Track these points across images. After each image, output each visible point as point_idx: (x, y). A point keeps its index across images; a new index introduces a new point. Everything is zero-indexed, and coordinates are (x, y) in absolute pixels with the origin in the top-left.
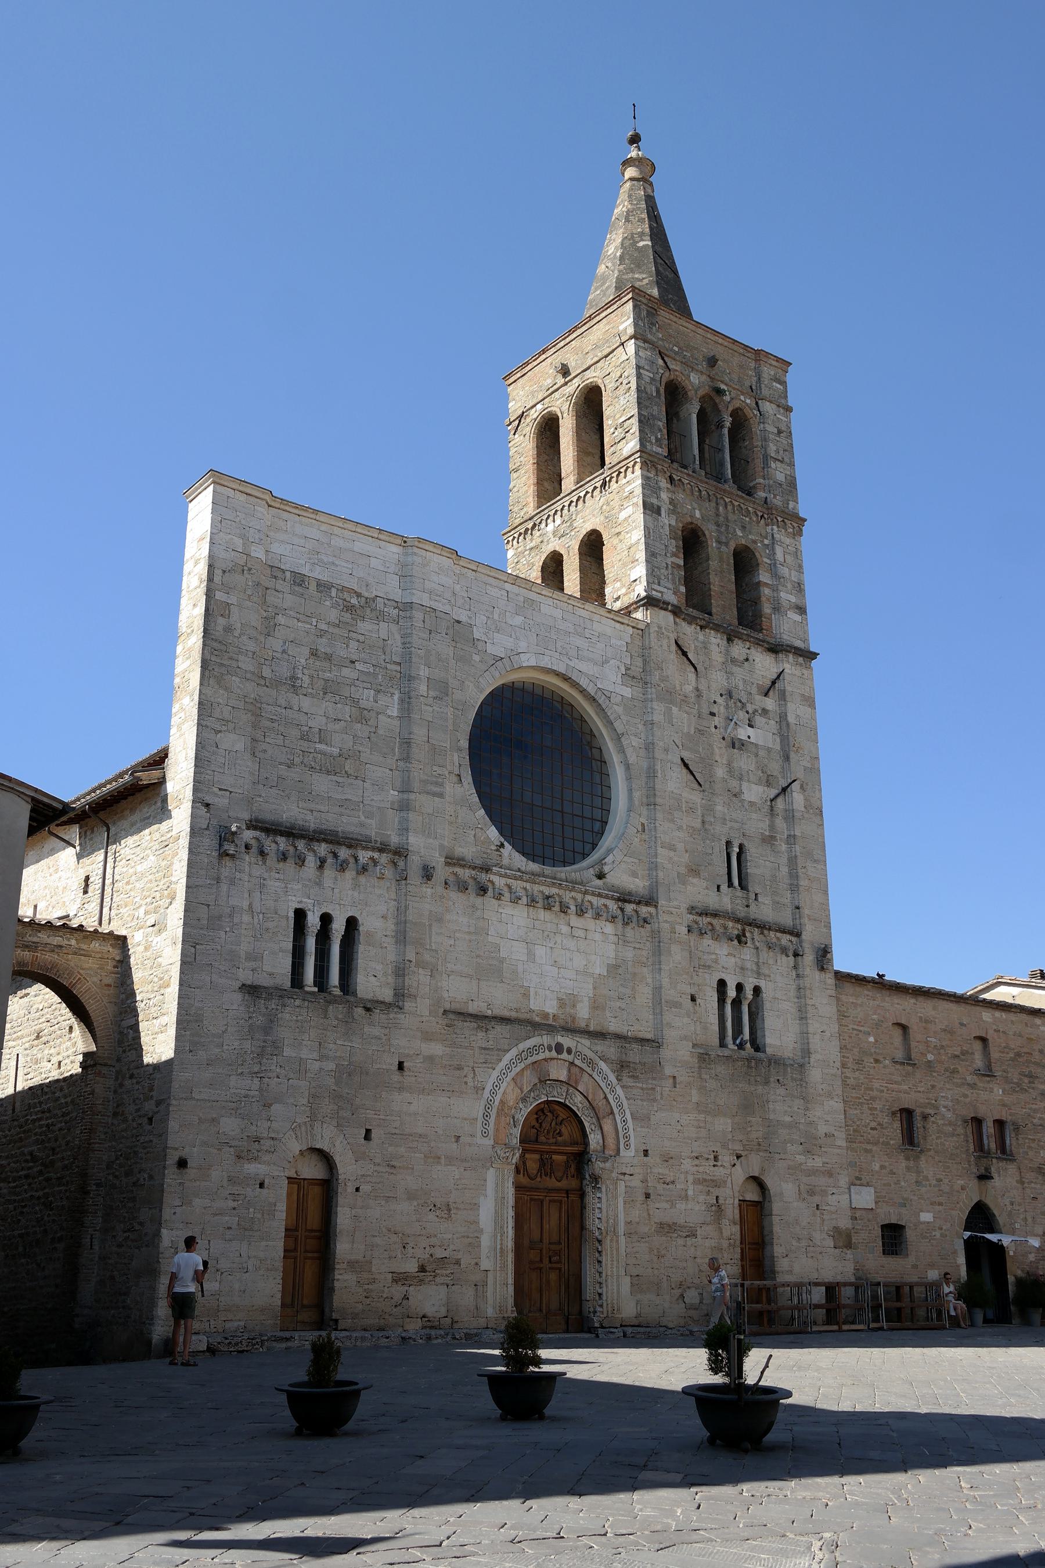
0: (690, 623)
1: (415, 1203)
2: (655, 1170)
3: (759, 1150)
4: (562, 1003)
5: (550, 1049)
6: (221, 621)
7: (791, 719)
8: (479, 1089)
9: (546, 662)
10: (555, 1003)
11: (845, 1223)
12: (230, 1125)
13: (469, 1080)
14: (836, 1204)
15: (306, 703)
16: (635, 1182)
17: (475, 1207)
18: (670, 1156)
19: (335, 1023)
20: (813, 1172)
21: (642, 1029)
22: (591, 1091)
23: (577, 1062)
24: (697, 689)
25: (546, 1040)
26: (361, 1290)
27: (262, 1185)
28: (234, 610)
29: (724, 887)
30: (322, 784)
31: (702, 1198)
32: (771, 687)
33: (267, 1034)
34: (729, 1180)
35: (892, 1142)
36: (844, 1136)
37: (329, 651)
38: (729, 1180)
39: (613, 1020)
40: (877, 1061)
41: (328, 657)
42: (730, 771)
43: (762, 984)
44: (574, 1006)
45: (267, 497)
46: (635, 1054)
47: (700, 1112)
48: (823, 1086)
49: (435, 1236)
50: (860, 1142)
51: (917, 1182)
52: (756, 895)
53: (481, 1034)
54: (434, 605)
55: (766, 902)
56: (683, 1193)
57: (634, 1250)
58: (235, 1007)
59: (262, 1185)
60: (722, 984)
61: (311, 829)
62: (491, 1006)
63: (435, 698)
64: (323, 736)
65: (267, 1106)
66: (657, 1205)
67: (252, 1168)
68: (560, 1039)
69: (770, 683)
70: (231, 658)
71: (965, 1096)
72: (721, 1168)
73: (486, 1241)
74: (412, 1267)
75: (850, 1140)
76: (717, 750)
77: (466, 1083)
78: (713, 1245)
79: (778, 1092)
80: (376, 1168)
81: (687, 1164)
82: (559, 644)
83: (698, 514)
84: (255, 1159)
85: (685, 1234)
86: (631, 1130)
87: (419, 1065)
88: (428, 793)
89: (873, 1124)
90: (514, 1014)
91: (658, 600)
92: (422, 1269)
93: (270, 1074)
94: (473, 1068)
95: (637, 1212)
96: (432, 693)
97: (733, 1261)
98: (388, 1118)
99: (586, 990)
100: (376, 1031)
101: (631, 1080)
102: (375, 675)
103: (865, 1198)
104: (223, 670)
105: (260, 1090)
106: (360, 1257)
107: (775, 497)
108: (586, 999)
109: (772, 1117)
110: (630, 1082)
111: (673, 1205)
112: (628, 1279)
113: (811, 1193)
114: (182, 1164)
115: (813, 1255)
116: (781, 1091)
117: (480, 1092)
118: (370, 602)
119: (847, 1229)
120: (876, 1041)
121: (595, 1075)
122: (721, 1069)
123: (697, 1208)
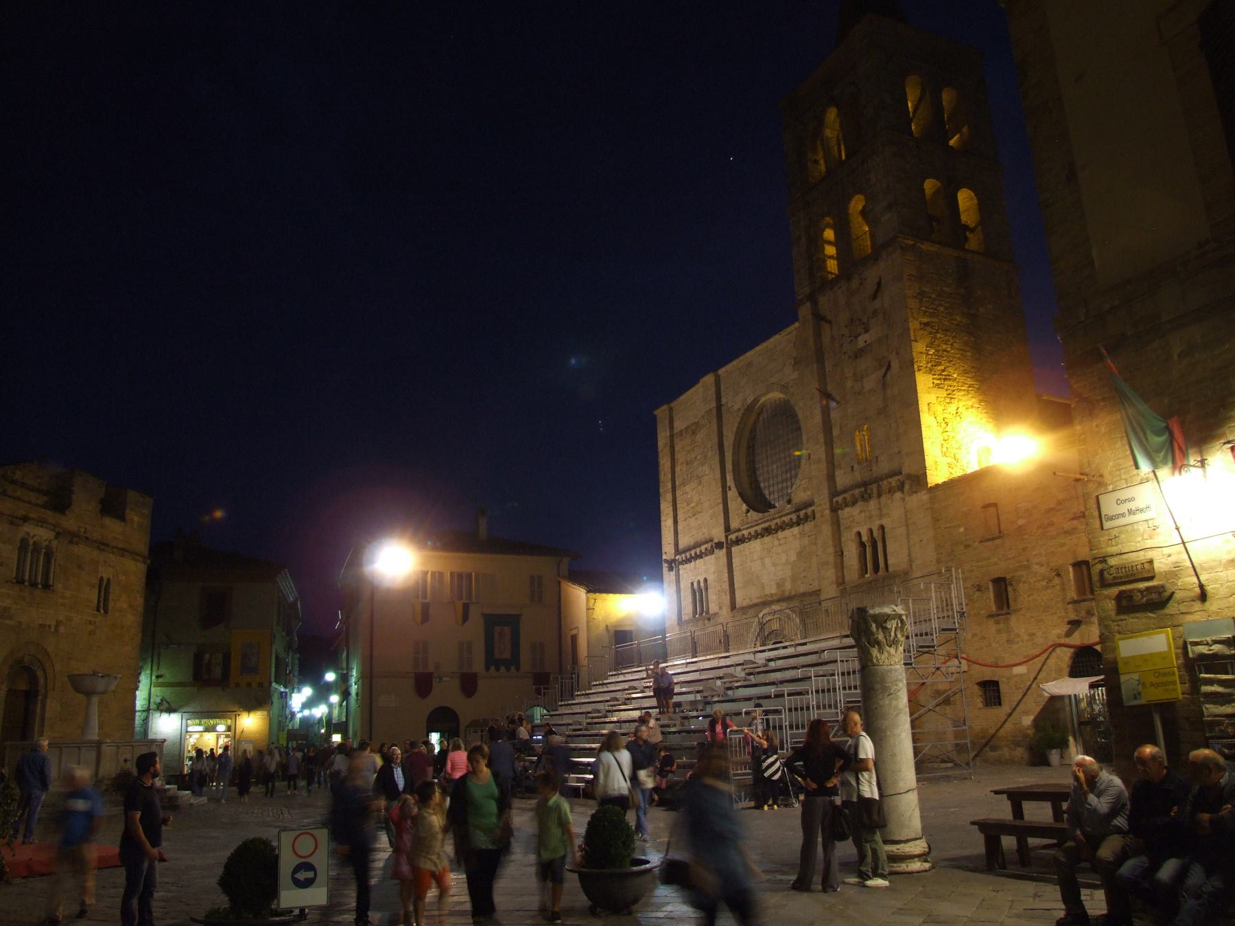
4: (779, 585)
40: (967, 546)
43: (884, 522)
51: (1008, 641)
60: (859, 534)
69: (875, 287)
71: (1063, 545)
108: (788, 579)
120: (966, 529)
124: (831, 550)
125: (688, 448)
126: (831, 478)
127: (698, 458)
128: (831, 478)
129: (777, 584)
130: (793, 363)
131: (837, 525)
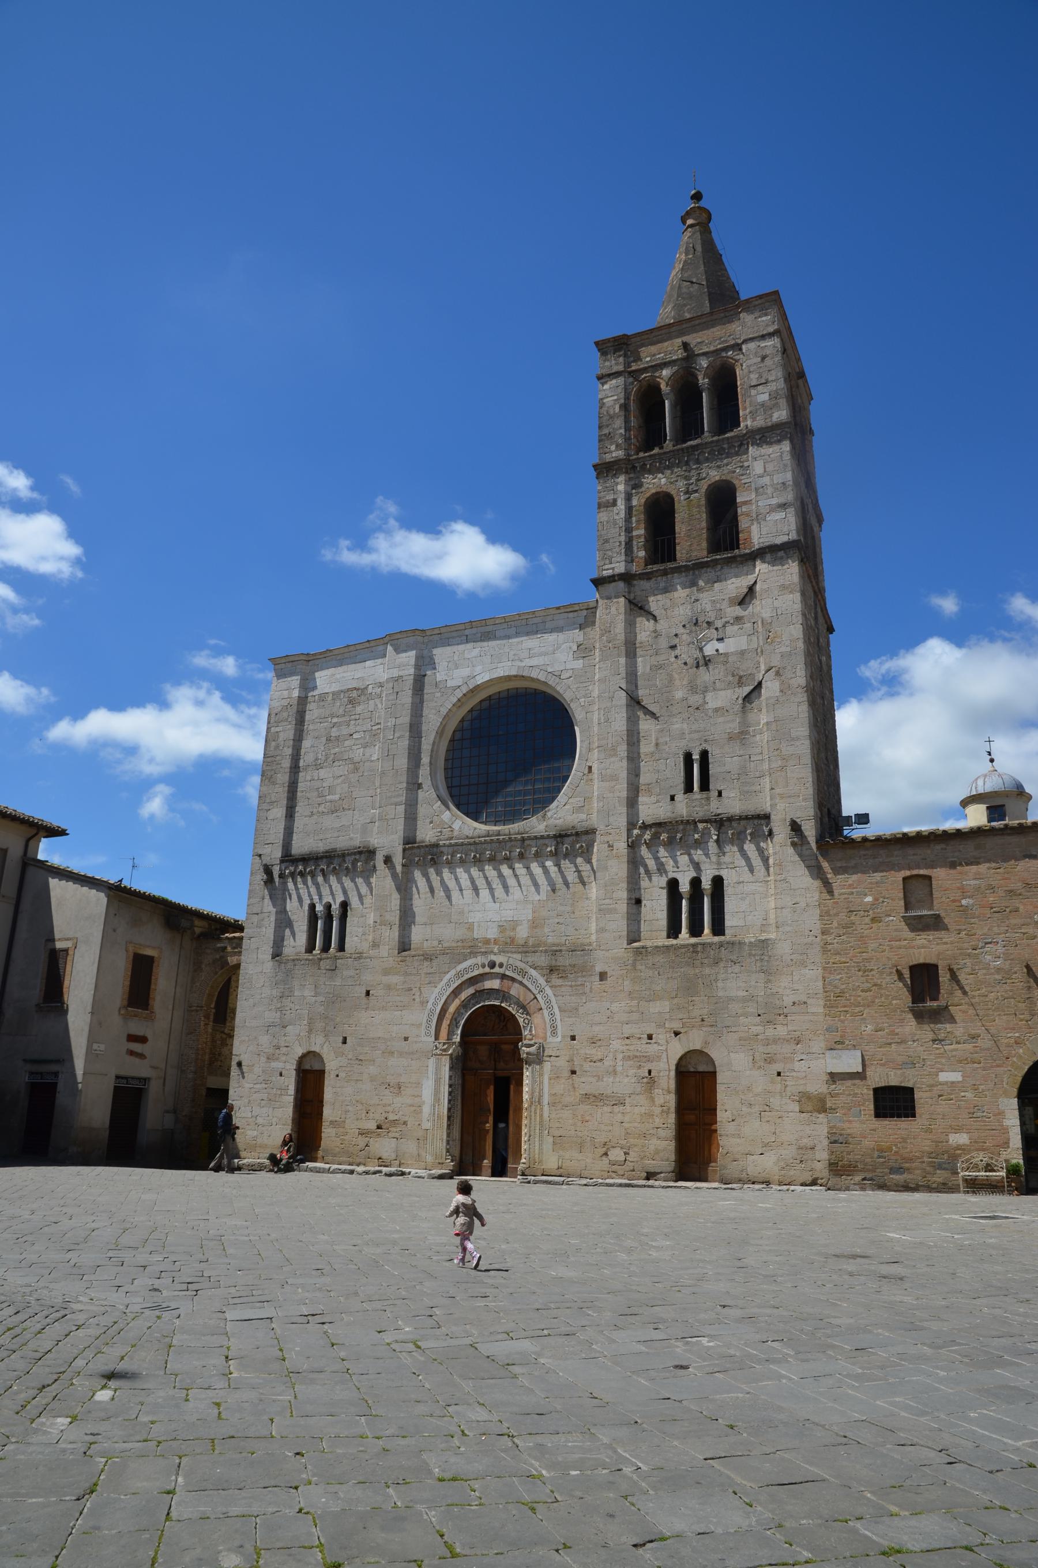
0: (649, 579)
1: (375, 1084)
2: (582, 1052)
3: (701, 1026)
4: (502, 928)
5: (483, 966)
6: (273, 744)
7: (766, 614)
8: (424, 1003)
9: (500, 673)
10: (495, 930)
11: (818, 1086)
12: (265, 1040)
13: (417, 997)
14: (804, 1069)
15: (322, 773)
16: (562, 1063)
17: (418, 1084)
18: (597, 1038)
19: (324, 971)
20: (775, 1041)
21: (580, 937)
22: (522, 993)
23: (507, 973)
24: (655, 631)
25: (479, 960)
26: (338, 1139)
27: (281, 1075)
28: (281, 734)
29: (680, 797)
30: (329, 821)
31: (631, 1072)
32: (746, 595)
33: (285, 984)
34: (664, 1056)
35: (894, 1002)
36: (822, 1003)
37: (337, 734)
38: (664, 1056)
39: (551, 934)
41: (337, 738)
42: (693, 689)
43: (724, 873)
44: (514, 929)
45: (302, 657)
46: (564, 961)
47: (632, 999)
48: (793, 957)
49: (390, 1105)
50: (845, 1007)
52: (720, 794)
53: (426, 963)
54: (401, 673)
55: (733, 795)
56: (611, 1069)
57: (558, 1116)
58: (269, 971)
59: (281, 1075)
61: (321, 851)
62: (442, 942)
63: (399, 738)
64: (331, 789)
65: (285, 1027)
66: (583, 1080)
67: (277, 1065)
68: (493, 957)
69: (746, 590)
70: (277, 764)
72: (656, 1045)
73: (426, 1110)
74: (372, 1125)
75: (829, 1006)
76: (676, 676)
77: (414, 1000)
78: (643, 1111)
79: (730, 970)
80: (349, 1061)
81: (616, 1044)
82: (512, 653)
83: (663, 481)
84: (277, 1059)
85: (612, 1103)
86: (558, 1020)
87: (380, 991)
88: (392, 804)
89: (866, 985)
90: (459, 944)
91: (613, 576)
92: (379, 1127)
93: (287, 1009)
94: (420, 988)
95: (562, 1086)
96: (397, 735)
97: (665, 1125)
98: (358, 1028)
99: (526, 914)
100: (352, 973)
101: (560, 980)
102: (365, 738)
103: (849, 1062)
104: (273, 772)
105: (280, 1018)
106: (338, 1119)
107: (754, 419)
108: (526, 922)
109: (720, 994)
110: (559, 982)
111: (599, 1078)
112: (550, 1139)
113: (770, 1060)
114: (239, 1064)
115: (768, 1119)
116: (737, 968)
117: (424, 1005)
118: (362, 691)
119: (821, 1093)
120: (876, 899)
121: (525, 981)
122: (660, 959)
123: (626, 1080)
124: (623, 895)
125: (335, 720)
126: (632, 803)
127: (355, 736)
128: (632, 803)
129: (499, 926)
130: (575, 648)
131: (635, 863)
